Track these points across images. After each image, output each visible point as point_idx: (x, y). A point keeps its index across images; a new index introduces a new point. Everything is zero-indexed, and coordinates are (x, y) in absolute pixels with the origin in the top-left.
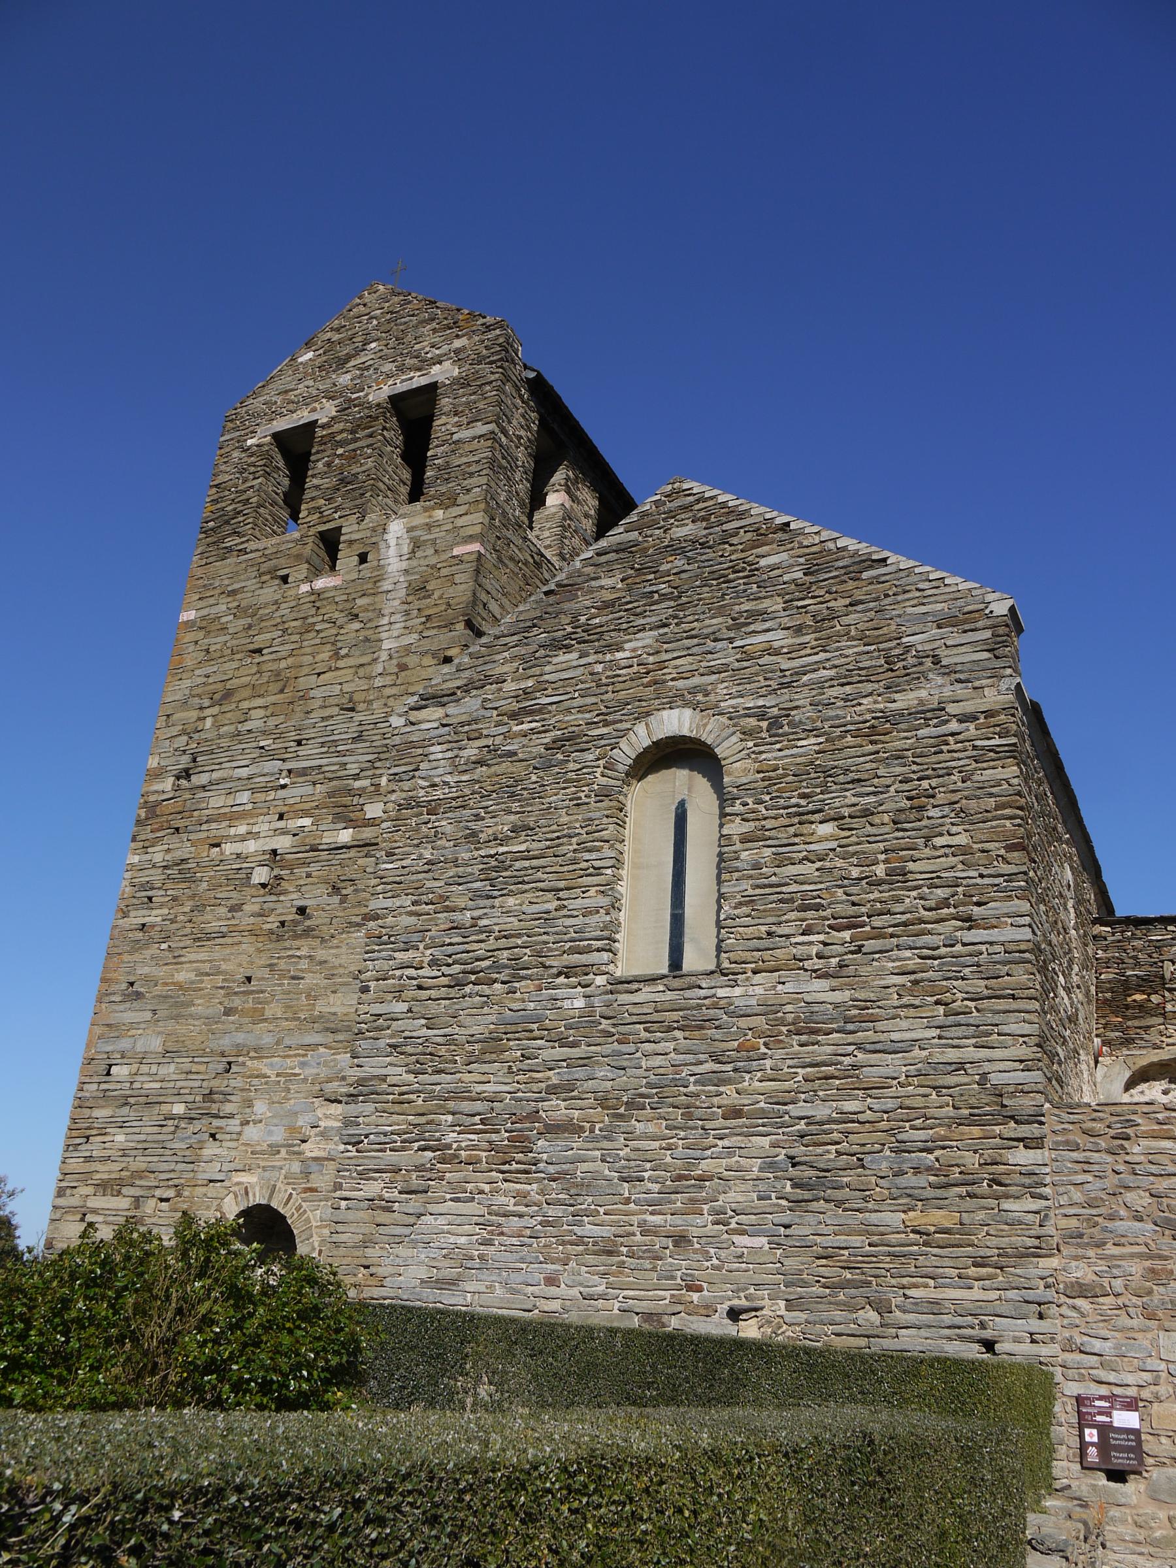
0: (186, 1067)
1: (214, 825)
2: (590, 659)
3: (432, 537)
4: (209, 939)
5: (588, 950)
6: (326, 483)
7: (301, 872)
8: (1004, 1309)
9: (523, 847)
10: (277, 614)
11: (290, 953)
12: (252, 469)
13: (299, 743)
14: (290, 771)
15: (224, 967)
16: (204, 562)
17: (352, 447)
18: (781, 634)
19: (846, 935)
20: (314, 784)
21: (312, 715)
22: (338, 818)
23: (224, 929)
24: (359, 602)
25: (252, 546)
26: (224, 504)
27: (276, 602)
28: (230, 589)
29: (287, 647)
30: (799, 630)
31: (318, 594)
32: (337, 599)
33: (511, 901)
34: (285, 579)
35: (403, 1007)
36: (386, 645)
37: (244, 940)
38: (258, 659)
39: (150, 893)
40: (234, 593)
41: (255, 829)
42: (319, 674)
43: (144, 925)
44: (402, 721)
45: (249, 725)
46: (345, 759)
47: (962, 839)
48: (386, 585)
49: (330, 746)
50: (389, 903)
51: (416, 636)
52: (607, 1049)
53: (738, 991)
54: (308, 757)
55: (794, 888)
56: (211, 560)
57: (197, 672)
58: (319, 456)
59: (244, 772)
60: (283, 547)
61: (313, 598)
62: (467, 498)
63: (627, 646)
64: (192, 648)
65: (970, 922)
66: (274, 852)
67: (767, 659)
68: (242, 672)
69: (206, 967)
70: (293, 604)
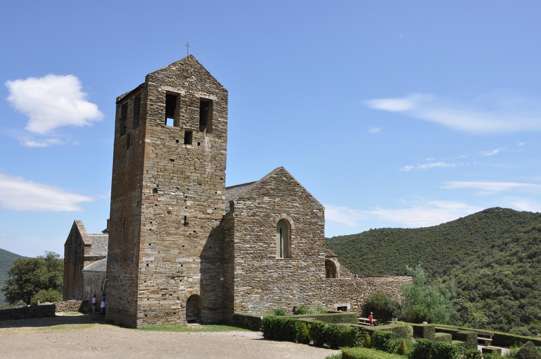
0: (171, 265)
1: (167, 206)
2: (271, 200)
3: (216, 145)
4: (171, 235)
6: (186, 116)
7: (193, 223)
8: (321, 303)
9: (262, 234)
10: (177, 151)
11: (193, 241)
12: (162, 100)
13: (188, 189)
14: (186, 197)
15: (177, 242)
16: (151, 125)
17: (192, 108)
20: (193, 201)
21: (190, 183)
22: (200, 211)
23: (175, 233)
24: (200, 156)
26: (154, 108)
28: (161, 137)
29: (181, 162)
30: (300, 204)
32: (193, 153)
34: (177, 141)
35: (243, 261)
36: (208, 170)
37: (181, 237)
38: (173, 163)
39: (151, 221)
40: (163, 139)
41: (180, 209)
42: (191, 173)
43: (151, 230)
45: (172, 181)
46: (201, 197)
47: (319, 243)
48: (206, 154)
49: (197, 193)
50: (238, 241)
53: (294, 262)
54: (191, 194)
57: (154, 160)
58: (183, 106)
59: (174, 194)
60: (176, 131)
61: (187, 150)
63: (276, 199)
64: (151, 152)
65: (319, 255)
66: (185, 216)
67: (296, 208)
68: (169, 165)
69: (172, 242)
70: (182, 150)
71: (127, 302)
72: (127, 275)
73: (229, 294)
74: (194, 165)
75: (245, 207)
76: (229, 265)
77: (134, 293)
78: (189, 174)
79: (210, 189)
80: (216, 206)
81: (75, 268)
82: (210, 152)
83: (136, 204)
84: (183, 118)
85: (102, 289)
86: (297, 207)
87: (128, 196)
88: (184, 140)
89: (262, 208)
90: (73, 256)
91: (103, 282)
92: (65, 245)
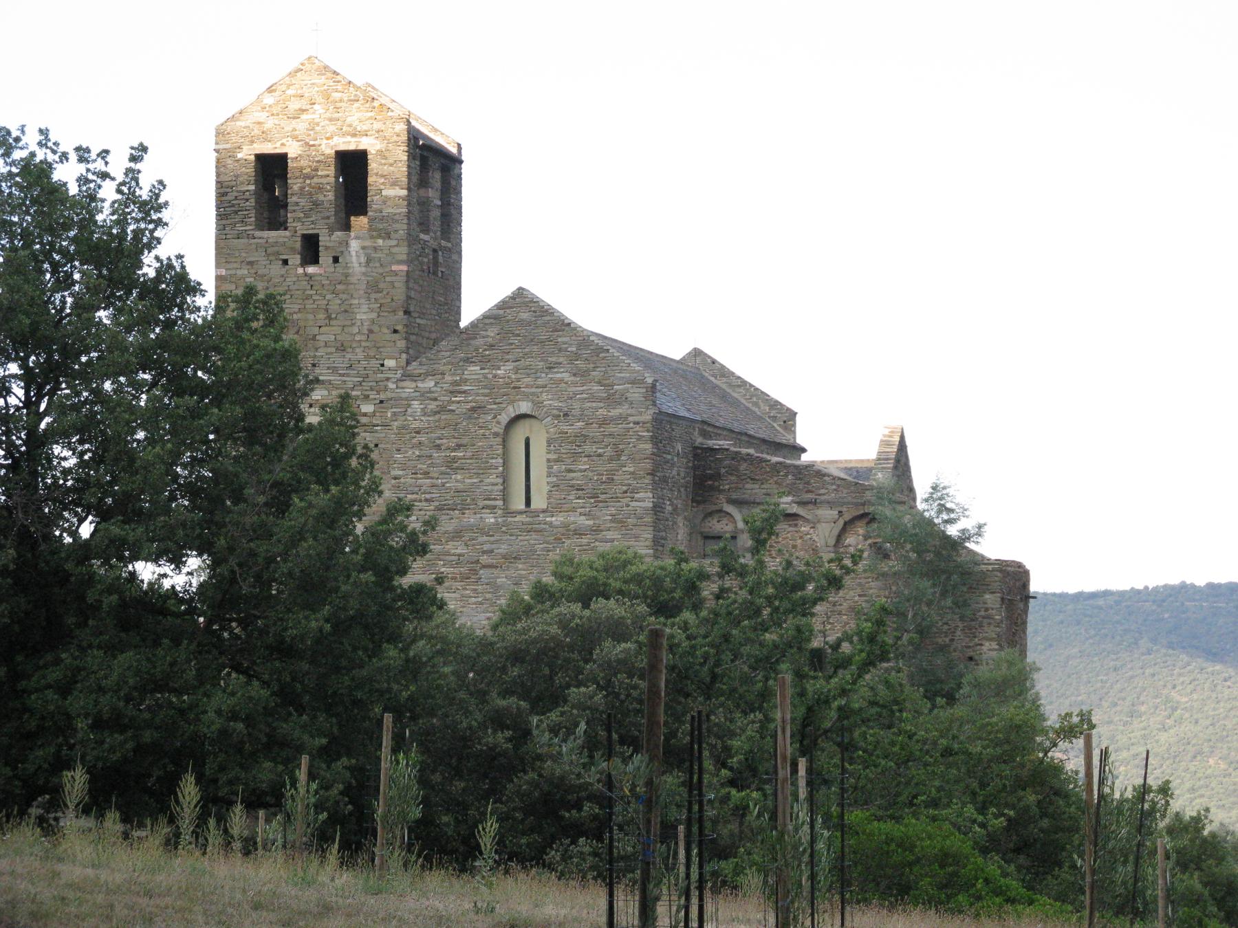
2: (486, 371)
5: (495, 499)
6: (303, 202)
18: (568, 374)
19: (592, 501)
24: (339, 287)
25: (258, 233)
27: (282, 276)
30: (575, 375)
31: (310, 277)
33: (459, 477)
34: (285, 262)
40: (251, 263)
44: (394, 386)
47: (632, 470)
48: (353, 280)
49: (334, 370)
50: (401, 473)
51: (376, 314)
52: (505, 538)
53: (554, 519)
55: (574, 482)
56: (228, 236)
58: (295, 181)
60: (281, 240)
61: (307, 278)
62: (397, 236)
70: (295, 279)
74: (327, 310)
75: (417, 394)
78: (316, 330)
79: (368, 358)
80: (382, 396)
82: (364, 274)
84: (296, 208)
86: (562, 380)
88: (299, 256)
89: (460, 392)
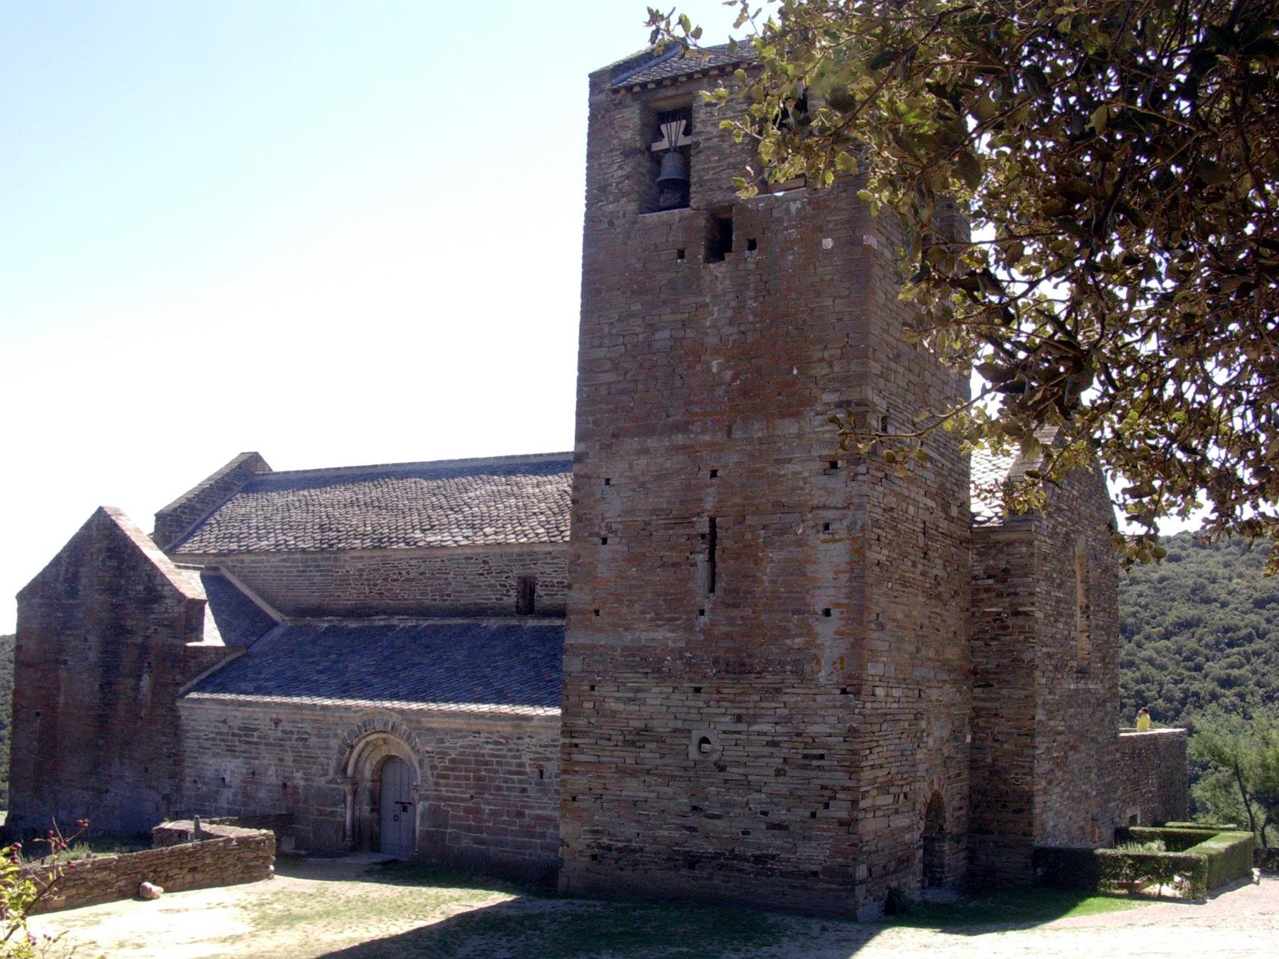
71: (763, 826)
72: (756, 728)
73: (1002, 787)
76: (1004, 692)
77: (827, 793)
81: (107, 686)
83: (818, 465)
85: (345, 770)
87: (737, 434)
90: (86, 640)
91: (352, 747)
92: (22, 597)
